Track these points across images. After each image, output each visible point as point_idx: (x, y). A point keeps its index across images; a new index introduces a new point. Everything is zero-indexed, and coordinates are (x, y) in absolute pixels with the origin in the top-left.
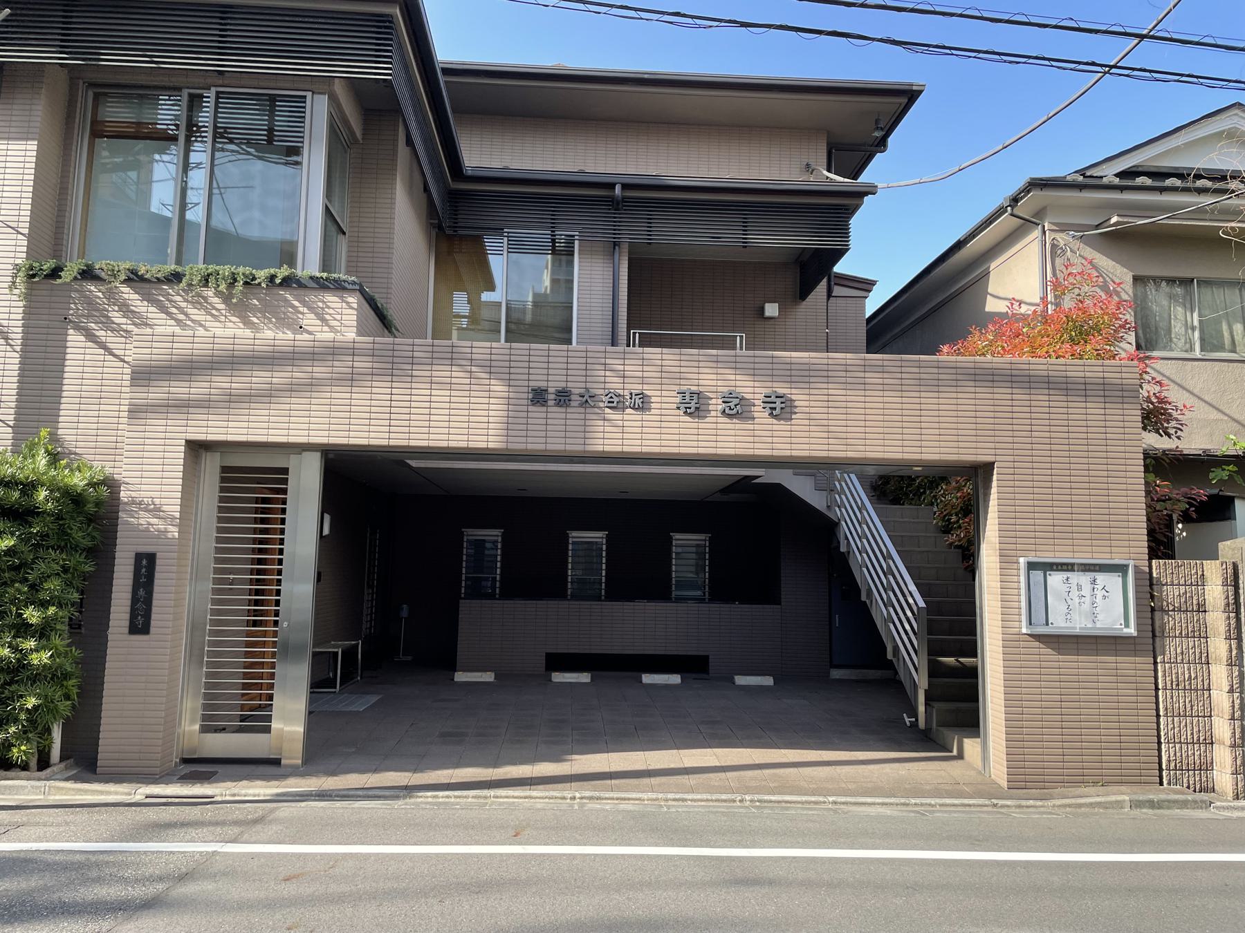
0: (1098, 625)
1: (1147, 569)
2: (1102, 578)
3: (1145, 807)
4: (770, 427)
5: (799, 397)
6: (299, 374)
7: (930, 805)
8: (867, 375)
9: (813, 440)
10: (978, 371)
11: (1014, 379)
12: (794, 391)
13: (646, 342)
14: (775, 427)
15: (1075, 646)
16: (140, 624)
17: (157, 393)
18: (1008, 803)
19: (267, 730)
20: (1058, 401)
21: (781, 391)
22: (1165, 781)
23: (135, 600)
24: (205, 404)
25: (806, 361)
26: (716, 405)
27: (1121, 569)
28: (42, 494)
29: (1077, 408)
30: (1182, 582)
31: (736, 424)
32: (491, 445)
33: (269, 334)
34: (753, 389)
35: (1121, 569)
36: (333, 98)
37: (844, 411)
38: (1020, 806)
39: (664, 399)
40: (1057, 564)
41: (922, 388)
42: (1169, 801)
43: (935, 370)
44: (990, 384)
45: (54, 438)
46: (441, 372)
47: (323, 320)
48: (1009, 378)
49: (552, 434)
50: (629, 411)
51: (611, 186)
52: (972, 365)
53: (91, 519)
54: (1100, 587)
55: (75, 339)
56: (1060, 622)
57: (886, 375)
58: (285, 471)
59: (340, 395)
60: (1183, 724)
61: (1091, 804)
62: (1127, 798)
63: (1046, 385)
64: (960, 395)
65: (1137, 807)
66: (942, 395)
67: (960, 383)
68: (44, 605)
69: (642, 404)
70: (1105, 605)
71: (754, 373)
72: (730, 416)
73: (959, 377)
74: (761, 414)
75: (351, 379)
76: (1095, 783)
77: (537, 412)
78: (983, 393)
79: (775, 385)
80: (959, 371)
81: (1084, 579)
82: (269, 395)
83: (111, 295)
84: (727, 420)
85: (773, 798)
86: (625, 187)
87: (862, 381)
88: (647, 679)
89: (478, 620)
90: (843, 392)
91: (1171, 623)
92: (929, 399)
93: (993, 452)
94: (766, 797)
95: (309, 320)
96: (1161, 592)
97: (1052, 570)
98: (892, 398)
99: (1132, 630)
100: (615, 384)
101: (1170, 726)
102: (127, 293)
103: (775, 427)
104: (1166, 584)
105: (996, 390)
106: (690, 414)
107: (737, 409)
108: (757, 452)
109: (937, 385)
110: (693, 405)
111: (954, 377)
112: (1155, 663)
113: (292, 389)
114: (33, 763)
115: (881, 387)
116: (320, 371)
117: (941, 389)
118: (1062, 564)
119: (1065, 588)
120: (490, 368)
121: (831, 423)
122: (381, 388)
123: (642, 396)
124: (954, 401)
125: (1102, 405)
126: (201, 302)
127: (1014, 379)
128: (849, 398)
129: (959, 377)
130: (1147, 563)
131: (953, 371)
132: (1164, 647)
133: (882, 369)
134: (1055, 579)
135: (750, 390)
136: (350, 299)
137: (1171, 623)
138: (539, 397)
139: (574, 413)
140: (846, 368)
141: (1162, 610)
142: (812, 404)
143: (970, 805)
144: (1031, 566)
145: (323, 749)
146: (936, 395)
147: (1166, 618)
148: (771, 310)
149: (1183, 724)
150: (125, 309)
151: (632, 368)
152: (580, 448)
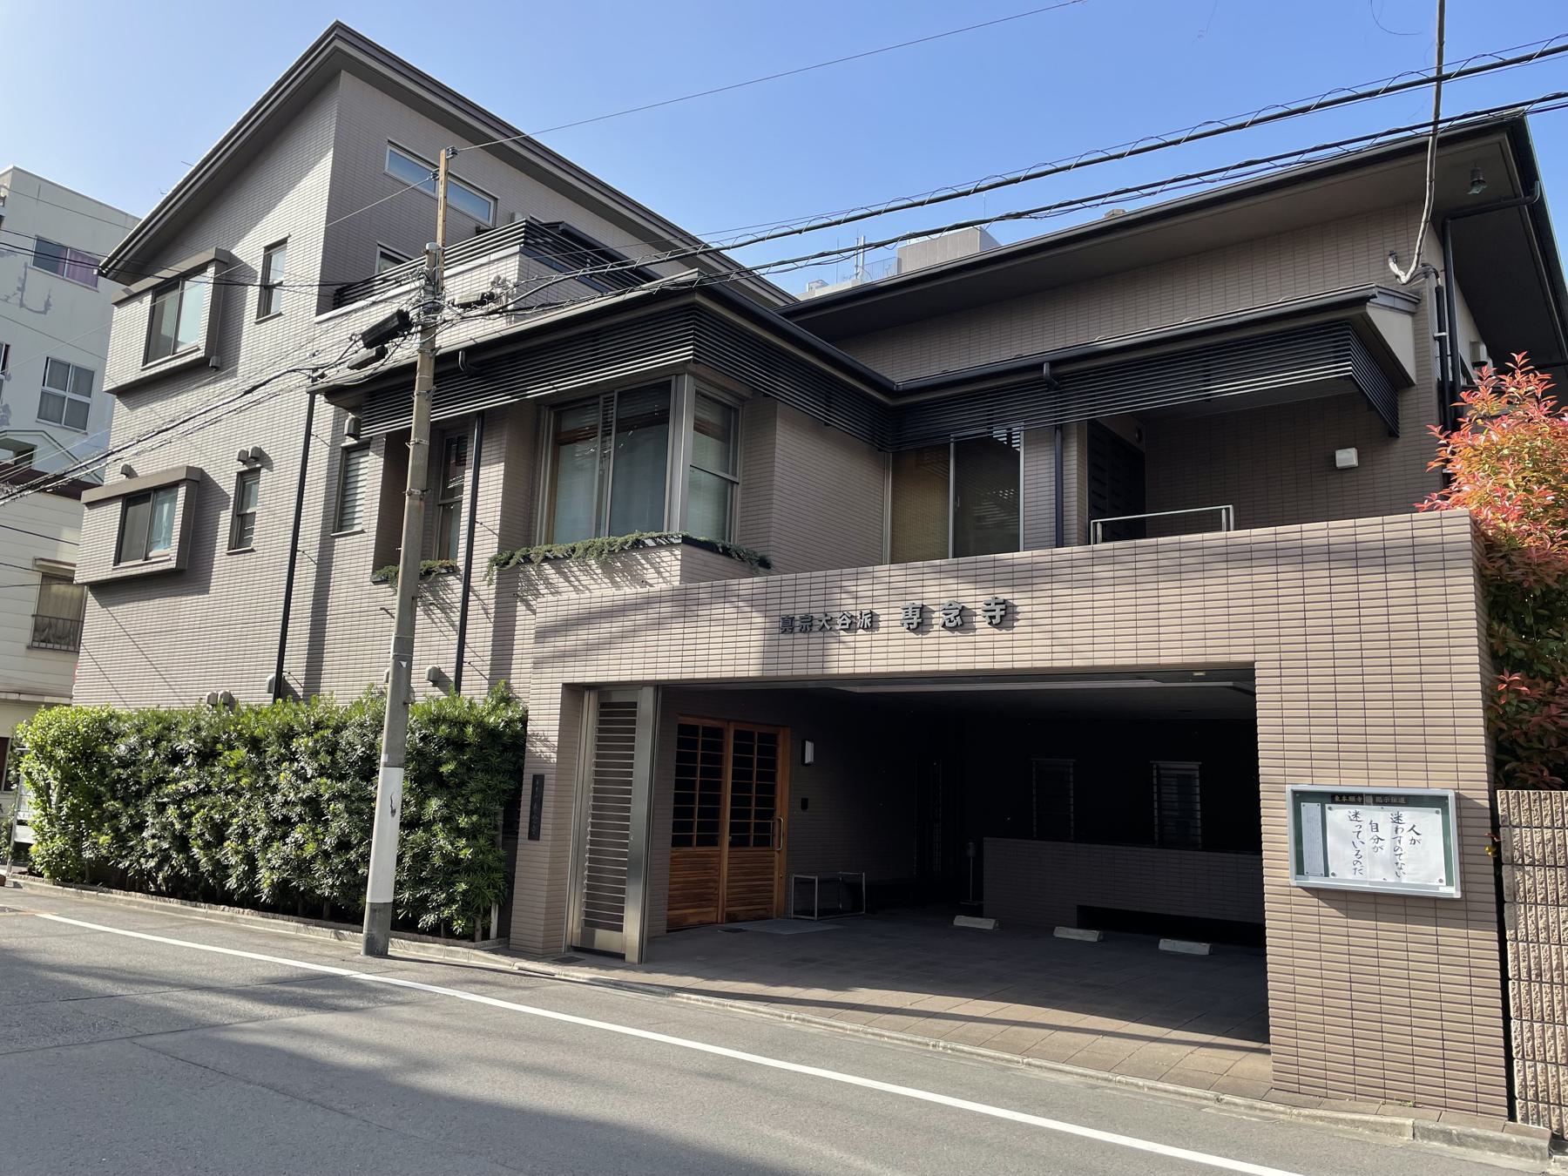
0: (1404, 880)
1: (1486, 804)
2: (1408, 815)
3: (1436, 1139)
4: (990, 638)
5: (1021, 601)
6: (627, 623)
7: (1137, 1086)
8: (1096, 569)
9: (1036, 650)
10: (1230, 549)
11: (1280, 553)
12: (1016, 596)
13: (1112, 534)
14: (997, 638)
15: (1432, 913)
16: (534, 835)
17: (548, 648)
18: (1238, 1100)
19: (620, 929)
20: (1344, 576)
21: (1002, 597)
22: (1519, 1117)
23: (532, 813)
24: (573, 654)
25: (1247, 540)
26: (938, 618)
27: (1438, 802)
28: (470, 730)
29: (1372, 582)
30: (1547, 822)
31: (959, 637)
32: (752, 674)
33: (628, 590)
34: (974, 597)
35: (1438, 802)
36: (692, 374)
37: (1069, 613)
38: (1251, 1107)
39: (892, 616)
40: (1341, 795)
41: (1161, 578)
42: (1477, 1138)
43: (1177, 554)
44: (1248, 563)
45: (508, 686)
46: (718, 610)
47: (659, 573)
48: (1273, 554)
49: (801, 662)
50: (860, 631)
51: (1039, 366)
52: (1223, 542)
53: (506, 748)
54: (1407, 827)
55: (521, 608)
56: (1345, 875)
57: (1117, 567)
58: (634, 705)
59: (651, 637)
60: (1549, 1034)
61: (1353, 1121)
62: (1410, 1122)
63: (1326, 557)
64: (1207, 582)
65: (1423, 1137)
66: (1184, 583)
67: (1207, 567)
68: (469, 813)
69: (873, 623)
70: (1419, 854)
71: (976, 580)
72: (951, 629)
73: (1207, 559)
74: (981, 622)
75: (659, 624)
76: (1403, 1101)
77: (786, 639)
78: (1239, 576)
79: (997, 590)
80: (1206, 552)
81: (1382, 815)
82: (609, 643)
83: (540, 573)
84: (948, 633)
85: (966, 1048)
86: (1054, 364)
87: (1089, 576)
88: (1166, 945)
89: (1006, 861)
90: (1069, 592)
91: (1529, 883)
92: (1169, 590)
93: (1251, 649)
94: (961, 1047)
95: (650, 575)
96: (1512, 836)
97: (1334, 802)
98: (1125, 593)
99: (1454, 892)
100: (849, 605)
101: (1527, 1035)
102: (548, 568)
103: (997, 638)
104: (1519, 826)
105: (1255, 570)
106: (913, 630)
107: (961, 621)
108: (1099, 662)
109: (1178, 572)
110: (915, 621)
111: (1200, 560)
112: (1502, 942)
113: (623, 636)
114: (478, 935)
115: (1111, 582)
116: (640, 618)
117: (1184, 576)
118: (1348, 795)
119: (1353, 826)
120: (752, 602)
121: (1055, 628)
122: (677, 628)
123: (872, 615)
124: (1200, 590)
125: (1411, 575)
126: (587, 571)
127: (1280, 553)
128: (1075, 598)
129: (1207, 559)
130: (1486, 794)
131: (1199, 552)
132: (1516, 917)
133: (1113, 560)
134: (1339, 815)
135: (972, 599)
136: (677, 552)
137: (1529, 883)
138: (788, 625)
139: (816, 637)
140: (1072, 563)
141: (1513, 863)
142: (1035, 608)
143: (1185, 1095)
144: (1300, 797)
145: (654, 953)
146: (1177, 584)
147: (1519, 875)
148: (1347, 457)
149: (1549, 1034)
150: (548, 584)
151: (863, 588)
152: (819, 672)
